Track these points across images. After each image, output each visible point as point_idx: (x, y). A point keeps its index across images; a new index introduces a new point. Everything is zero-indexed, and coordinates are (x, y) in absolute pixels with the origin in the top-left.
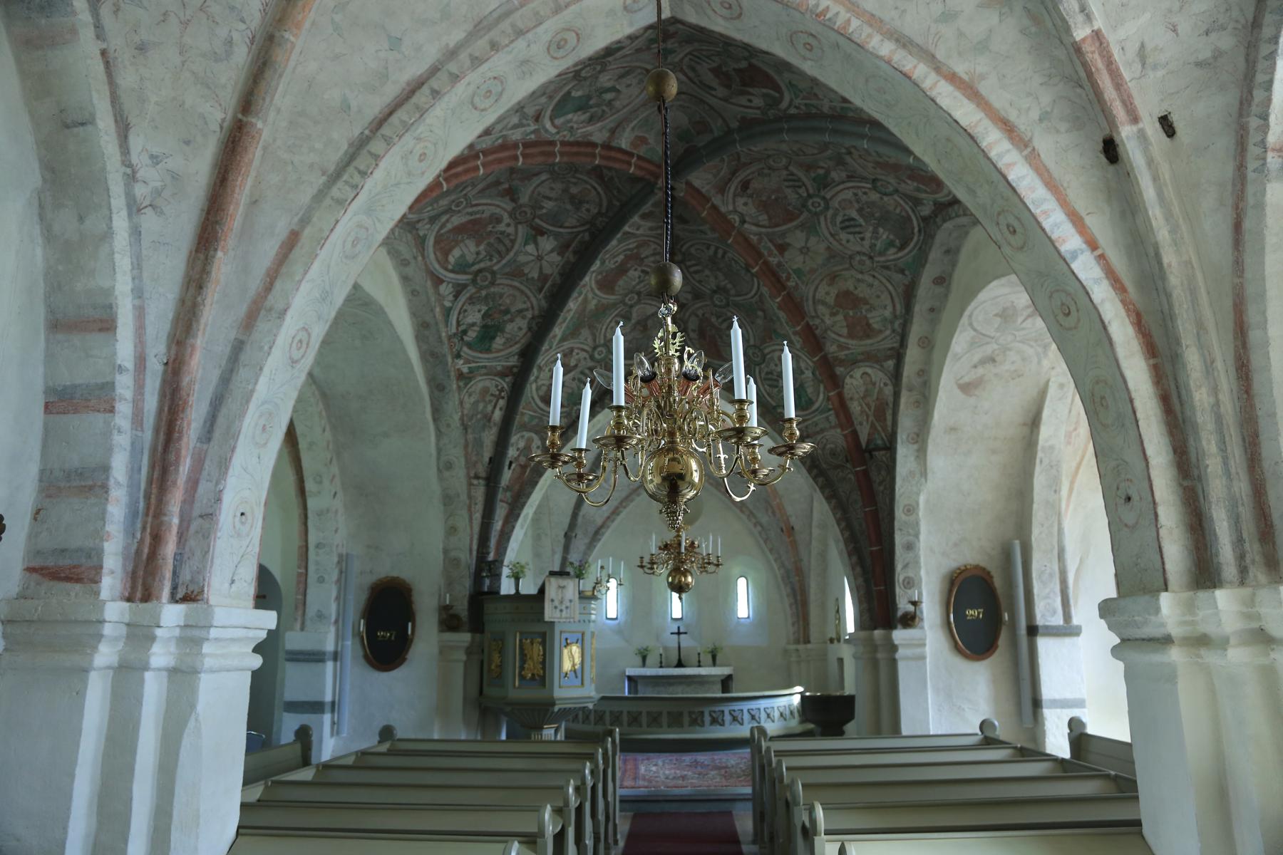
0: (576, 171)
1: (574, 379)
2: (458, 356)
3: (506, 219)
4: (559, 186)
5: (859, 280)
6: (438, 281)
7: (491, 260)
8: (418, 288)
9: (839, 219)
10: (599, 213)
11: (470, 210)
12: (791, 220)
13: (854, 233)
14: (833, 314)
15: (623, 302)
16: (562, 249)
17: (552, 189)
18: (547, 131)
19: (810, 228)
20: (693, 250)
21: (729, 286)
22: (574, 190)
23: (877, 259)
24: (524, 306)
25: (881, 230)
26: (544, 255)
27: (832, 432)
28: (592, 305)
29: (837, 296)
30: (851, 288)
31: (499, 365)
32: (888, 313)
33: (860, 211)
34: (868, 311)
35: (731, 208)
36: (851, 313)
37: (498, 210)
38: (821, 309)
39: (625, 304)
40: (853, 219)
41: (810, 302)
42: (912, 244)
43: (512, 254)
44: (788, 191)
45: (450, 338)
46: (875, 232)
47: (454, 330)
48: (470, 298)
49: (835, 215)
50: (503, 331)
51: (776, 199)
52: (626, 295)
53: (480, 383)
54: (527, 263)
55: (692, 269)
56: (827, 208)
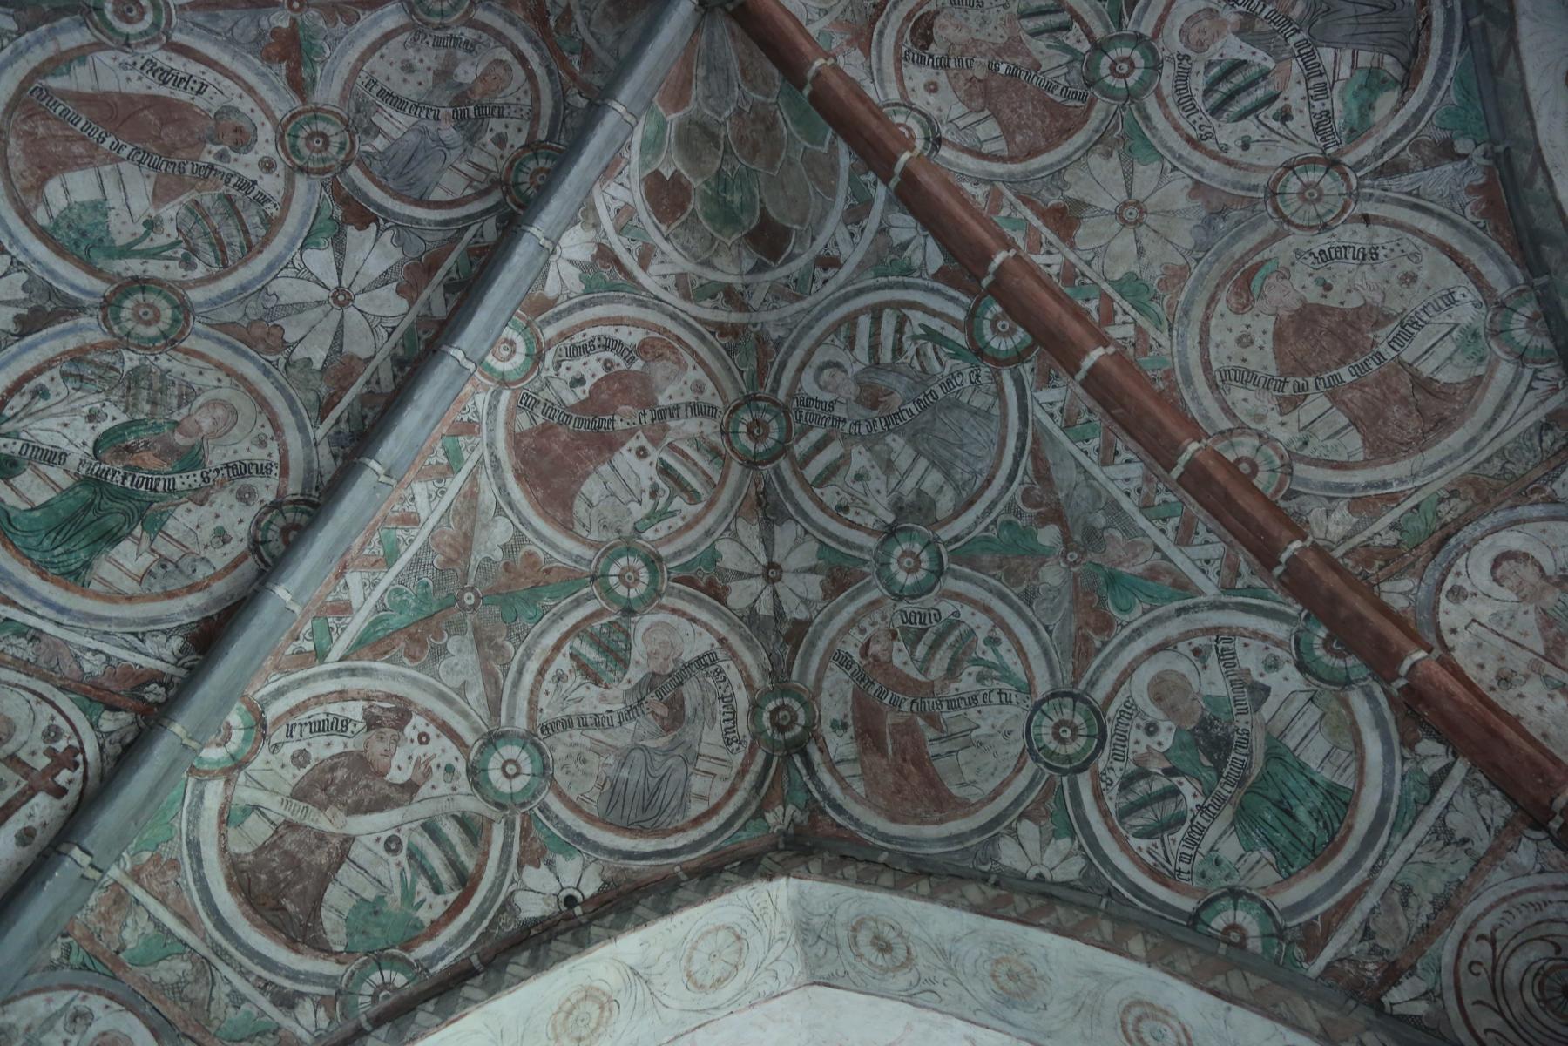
1: (392, 845)
3: (265, 145)
4: (428, 58)
5: (1324, 257)
7: (187, 263)
9: (1198, 83)
10: (532, 146)
11: (162, 58)
12: (1067, 133)
13: (1253, 110)
14: (1290, 404)
16: (413, 276)
17: (408, 68)
19: (1128, 141)
20: (808, 385)
21: (935, 477)
22: (467, 72)
23: (1349, 159)
24: (258, 455)
25: (1326, 55)
27: (1498, 882)
28: (495, 537)
29: (1278, 337)
30: (1313, 295)
31: (97, 653)
32: (1468, 313)
33: (1244, 30)
34: (1398, 340)
35: (894, 95)
36: (1345, 374)
37: (247, 104)
38: (1237, 394)
39: (608, 591)
40: (1238, 65)
41: (1202, 387)
42: (1436, 43)
43: (259, 264)
44: (1039, 46)
46: (1312, 70)
48: (77, 357)
49: (1182, 79)
50: (155, 526)
51: (1013, 73)
52: (612, 554)
54: (300, 308)
55: (811, 472)
56: (1155, 66)
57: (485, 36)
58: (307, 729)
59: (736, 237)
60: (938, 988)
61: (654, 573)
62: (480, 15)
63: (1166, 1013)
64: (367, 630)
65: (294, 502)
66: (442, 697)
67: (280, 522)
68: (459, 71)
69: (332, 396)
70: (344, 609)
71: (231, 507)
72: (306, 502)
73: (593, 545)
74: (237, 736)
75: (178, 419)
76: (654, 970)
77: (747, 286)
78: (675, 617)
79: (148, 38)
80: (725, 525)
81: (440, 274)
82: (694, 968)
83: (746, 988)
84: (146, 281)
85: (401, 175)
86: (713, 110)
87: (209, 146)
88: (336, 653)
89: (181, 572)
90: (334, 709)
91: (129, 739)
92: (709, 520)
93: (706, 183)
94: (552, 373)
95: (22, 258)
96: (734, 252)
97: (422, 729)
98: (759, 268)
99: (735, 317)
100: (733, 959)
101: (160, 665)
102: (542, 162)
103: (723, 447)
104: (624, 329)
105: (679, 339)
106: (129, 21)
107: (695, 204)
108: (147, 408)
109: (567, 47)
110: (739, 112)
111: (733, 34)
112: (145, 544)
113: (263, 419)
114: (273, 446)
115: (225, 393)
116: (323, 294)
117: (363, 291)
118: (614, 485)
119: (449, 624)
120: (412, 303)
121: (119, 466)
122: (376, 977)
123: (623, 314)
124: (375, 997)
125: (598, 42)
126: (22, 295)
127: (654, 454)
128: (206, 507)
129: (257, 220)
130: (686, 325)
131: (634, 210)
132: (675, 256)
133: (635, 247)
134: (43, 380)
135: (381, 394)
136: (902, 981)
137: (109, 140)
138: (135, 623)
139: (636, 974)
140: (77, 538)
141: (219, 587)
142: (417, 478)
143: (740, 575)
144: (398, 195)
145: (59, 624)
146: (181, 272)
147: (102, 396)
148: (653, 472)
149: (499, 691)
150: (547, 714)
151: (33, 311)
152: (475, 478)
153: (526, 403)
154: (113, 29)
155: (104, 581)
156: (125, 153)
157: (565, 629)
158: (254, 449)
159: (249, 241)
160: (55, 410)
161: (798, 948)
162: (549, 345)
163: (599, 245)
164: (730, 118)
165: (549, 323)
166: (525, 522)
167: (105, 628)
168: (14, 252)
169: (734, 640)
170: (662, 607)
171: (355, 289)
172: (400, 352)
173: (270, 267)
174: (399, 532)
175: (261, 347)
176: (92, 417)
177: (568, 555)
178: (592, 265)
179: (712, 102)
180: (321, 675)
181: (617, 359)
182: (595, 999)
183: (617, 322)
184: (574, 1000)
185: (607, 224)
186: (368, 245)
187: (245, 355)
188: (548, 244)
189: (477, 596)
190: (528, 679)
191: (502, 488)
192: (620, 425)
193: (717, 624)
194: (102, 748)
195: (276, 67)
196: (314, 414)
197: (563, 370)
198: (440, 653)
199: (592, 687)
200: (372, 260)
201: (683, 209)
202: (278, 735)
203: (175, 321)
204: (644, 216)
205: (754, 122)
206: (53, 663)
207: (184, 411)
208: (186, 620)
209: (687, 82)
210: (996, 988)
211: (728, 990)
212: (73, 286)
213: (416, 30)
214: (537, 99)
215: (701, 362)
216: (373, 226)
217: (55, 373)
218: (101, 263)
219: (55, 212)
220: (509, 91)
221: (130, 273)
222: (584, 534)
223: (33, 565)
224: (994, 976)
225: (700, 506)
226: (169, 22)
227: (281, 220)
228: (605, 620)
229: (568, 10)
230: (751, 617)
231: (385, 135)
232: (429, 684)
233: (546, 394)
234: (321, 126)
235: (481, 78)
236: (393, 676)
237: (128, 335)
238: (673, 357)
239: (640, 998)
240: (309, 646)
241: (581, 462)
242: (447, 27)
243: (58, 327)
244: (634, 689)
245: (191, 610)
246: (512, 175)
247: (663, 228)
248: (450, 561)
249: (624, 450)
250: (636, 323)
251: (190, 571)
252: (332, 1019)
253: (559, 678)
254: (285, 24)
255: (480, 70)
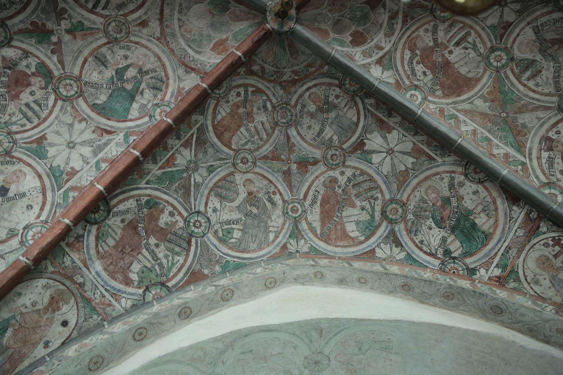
0: (287, 104)
2: (472, 272)
3: (336, 174)
4: (306, 121)
6: (370, 255)
7: (376, 199)
8: (355, 276)
15: (498, 70)
16: (384, 127)
17: (309, 127)
18: (138, 126)
22: (312, 108)
24: (446, 180)
26: (388, 149)
31: (516, 230)
37: (322, 179)
39: (503, 66)
45: (442, 270)
47: (437, 262)
48: (409, 232)
50: (470, 212)
52: (489, 65)
53: (529, 263)
54: (393, 165)
57: (300, 101)
58: (551, 170)
59: (372, 14)
61: (497, 49)
62: (293, 102)
64: (515, 149)
65: (465, 169)
66: (541, 126)
67: (472, 174)
68: (311, 110)
69: (426, 156)
70: (507, 156)
71: (465, 189)
72: (466, 165)
73: (485, 71)
74: (553, 191)
75: (431, 204)
77: (390, 11)
78: (516, 42)
79: (303, 206)
80: (480, 22)
81: (385, 119)
84: (382, 211)
85: (347, 131)
86: (329, 20)
87: (336, 190)
88: (523, 159)
89: (488, 205)
90: (544, 161)
91: (551, 223)
92: (478, 28)
93: (353, 24)
94: (422, 82)
95: (376, 244)
96: (377, 15)
97: (554, 133)
98: (384, 6)
99: (400, 16)
101: (523, 213)
102: (347, 82)
103: (449, 22)
104: (405, 56)
105: (408, 37)
106: (298, 210)
107: (360, 29)
108: (427, 213)
109: (306, 73)
110: (330, 11)
111: (304, 12)
112: (477, 216)
113: (433, 178)
114: (443, 175)
115: (423, 189)
116: (389, 158)
117: (388, 145)
118: (462, 62)
119: (513, 122)
120: (394, 129)
121: (448, 222)
123: (399, 57)
125: (305, 61)
126: (388, 245)
127: (451, 48)
128: (465, 197)
129: (361, 177)
130: (403, 34)
131: (363, 51)
132: (379, 37)
133: (376, 51)
134: (417, 241)
135: (427, 140)
137: (335, 219)
138: (506, 220)
140: (473, 235)
141: (495, 194)
142: (459, 129)
143: (501, 16)
144: (354, 133)
145: (504, 241)
146: (379, 201)
147: (423, 225)
148: (458, 48)
149: (540, 106)
150: (552, 90)
151: (393, 242)
152: (460, 110)
153: (432, 92)
154: (301, 215)
155: (490, 228)
156: (339, 215)
157: (517, 82)
158: (444, 181)
159: (369, 180)
160: (427, 238)
162: (411, 83)
163: (376, 63)
164: (332, 15)
165: (404, 82)
166: (476, 94)
167: (507, 229)
168: (374, 246)
169: (529, 19)
170: (512, 47)
171: (387, 147)
172: (412, 133)
173: (378, 174)
174: (479, 136)
175: (406, 178)
176: (430, 228)
177: (488, 80)
178: (383, 66)
179: (326, 21)
180: (531, 164)
181: (416, 59)
183: (402, 59)
185: (369, 60)
186: (371, 142)
187: (409, 183)
188: (379, 81)
189: (503, 112)
190: (536, 96)
191: (463, 101)
192: (440, 60)
193: (521, 26)
194: (553, 231)
195: (309, 169)
196: (433, 162)
197: (420, 78)
198: (524, 125)
199: (542, 73)
200: (377, 142)
201: (362, 33)
202: (553, 179)
203: (396, 203)
204: (365, 47)
205: (334, 5)
206: (519, 243)
207: (429, 202)
208: (507, 204)
209: (320, 30)
212: (385, 231)
213: (297, 124)
214: (323, 84)
215: (417, 29)
216: (365, 141)
217: (415, 238)
218: (376, 223)
219: (360, 235)
220: (320, 94)
221: (380, 215)
222: (480, 74)
223: (483, 247)
225: (472, 31)
226: (297, 199)
227: (362, 170)
228: (515, 68)
229: (293, 72)
230: (520, 12)
231: (333, 136)
232: (536, 130)
233: (429, 85)
234: (329, 156)
235: (314, 103)
236: (532, 141)
237: (401, 217)
238: (415, 39)
240: (520, 167)
241: (454, 74)
242: (296, 114)
243: (399, 236)
244: (545, 58)
245: (503, 203)
246: (350, 93)
247: (369, 41)
248: (489, 120)
249: (449, 59)
250: (403, 52)
251: (488, 203)
253: (537, 85)
254: (296, 165)
255: (311, 103)
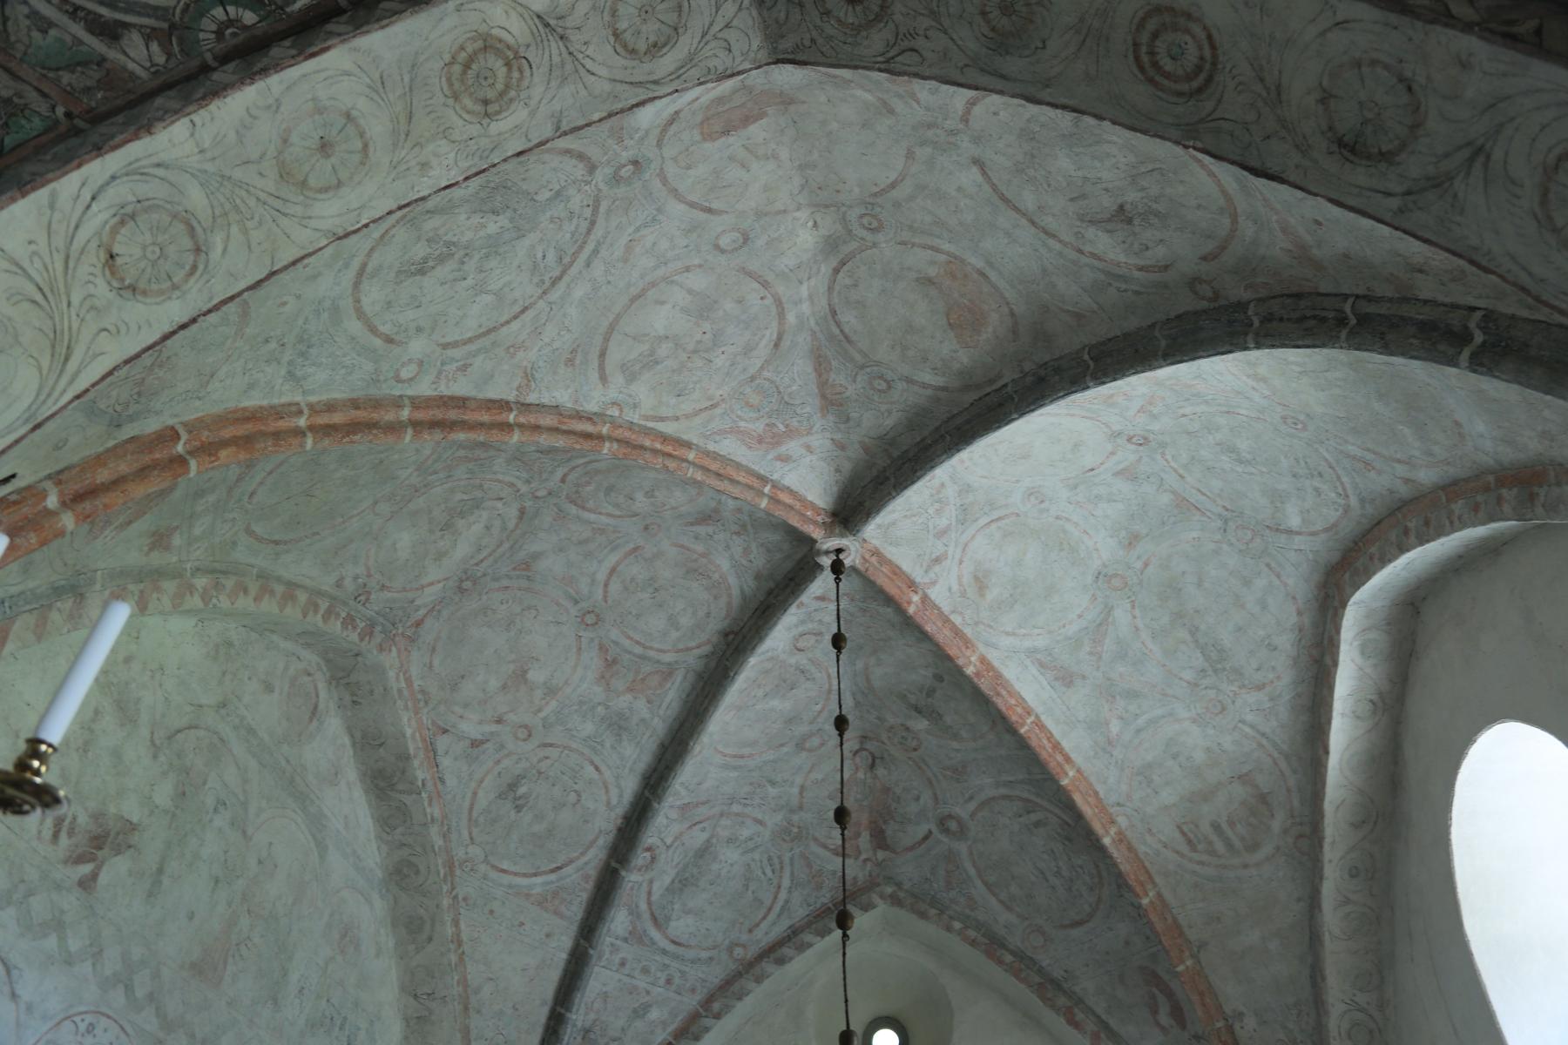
60: (920, 43)
63: (1189, 16)
76: (569, 22)
82: (622, 25)
83: (690, 60)
100: (671, 18)
122: (218, 12)
124: (219, 34)
136: (877, 40)
139: (547, 25)
161: (754, 13)
182: (498, 53)
184: (470, 49)
210: (986, 30)
211: (667, 62)
224: (984, 14)
239: (556, 59)
252: (169, 55)
